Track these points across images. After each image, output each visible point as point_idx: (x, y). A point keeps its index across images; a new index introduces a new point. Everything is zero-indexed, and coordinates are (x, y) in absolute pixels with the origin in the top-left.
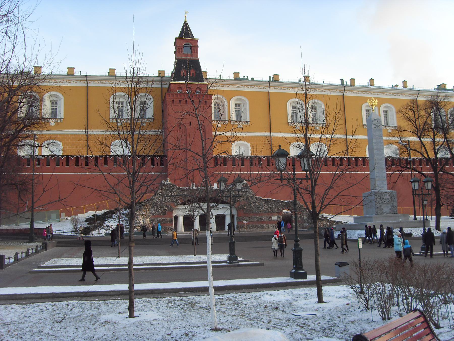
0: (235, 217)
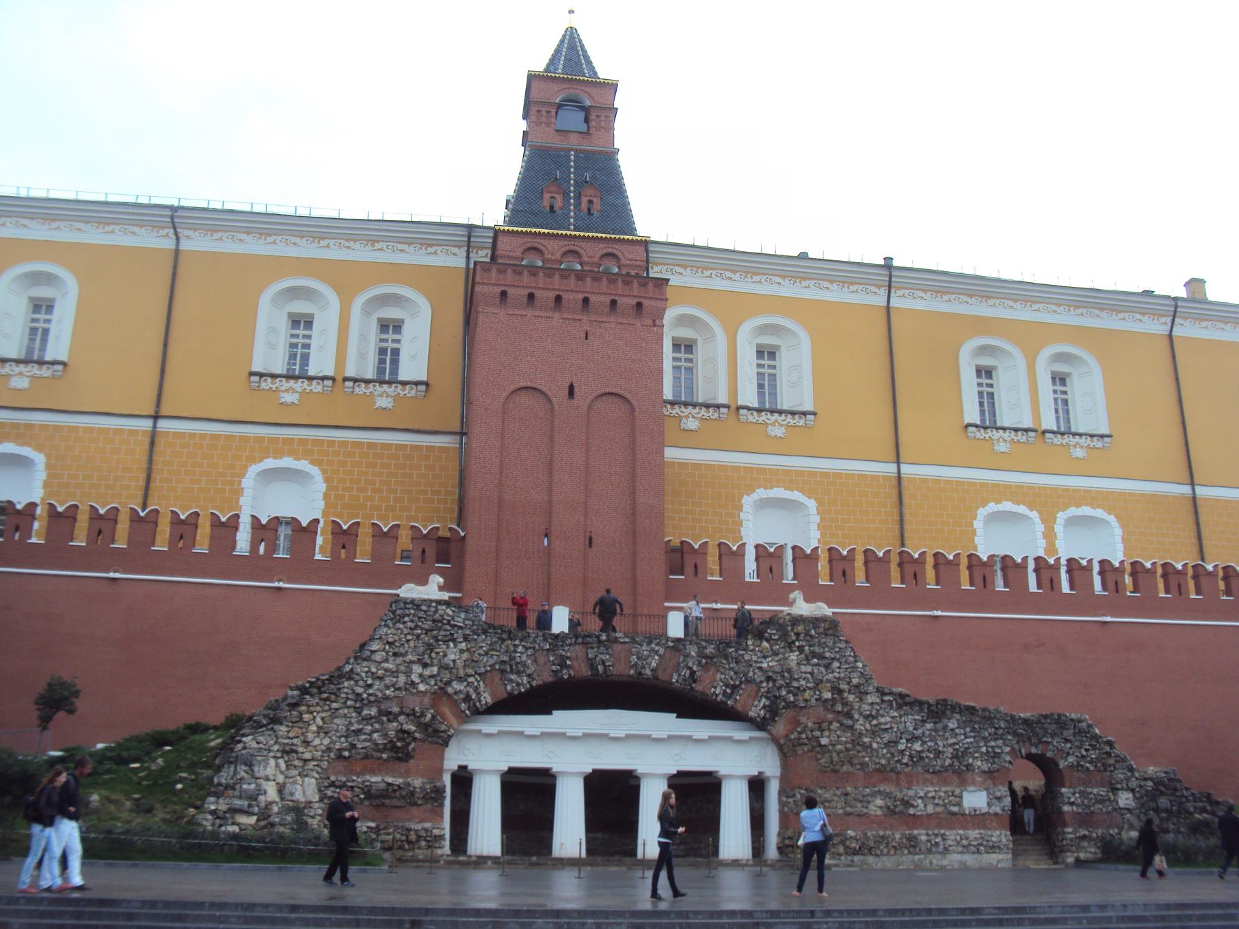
0: (773, 790)
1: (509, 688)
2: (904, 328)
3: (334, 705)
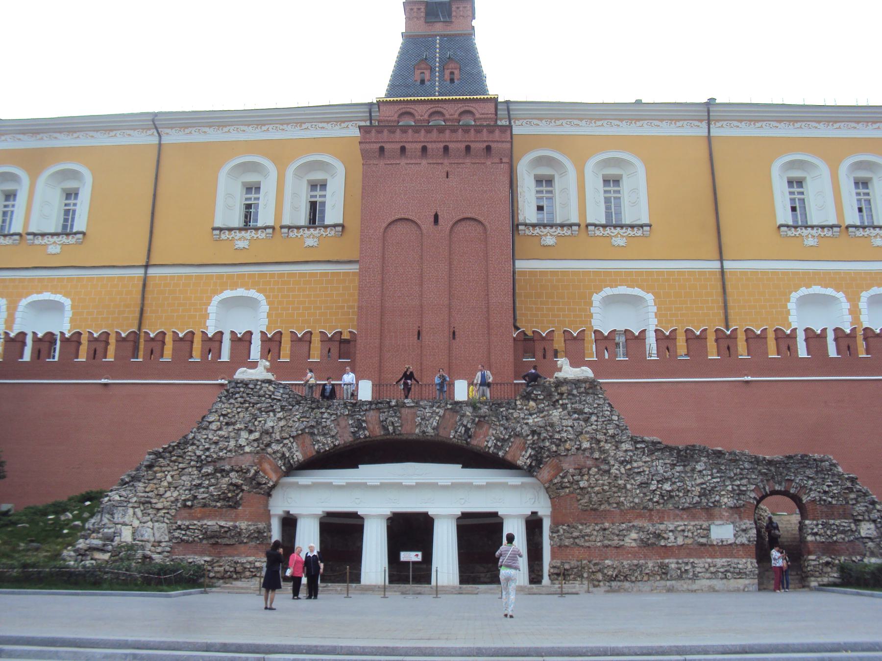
0: (547, 525)
1: (316, 447)
2: (712, 147)
3: (181, 466)
